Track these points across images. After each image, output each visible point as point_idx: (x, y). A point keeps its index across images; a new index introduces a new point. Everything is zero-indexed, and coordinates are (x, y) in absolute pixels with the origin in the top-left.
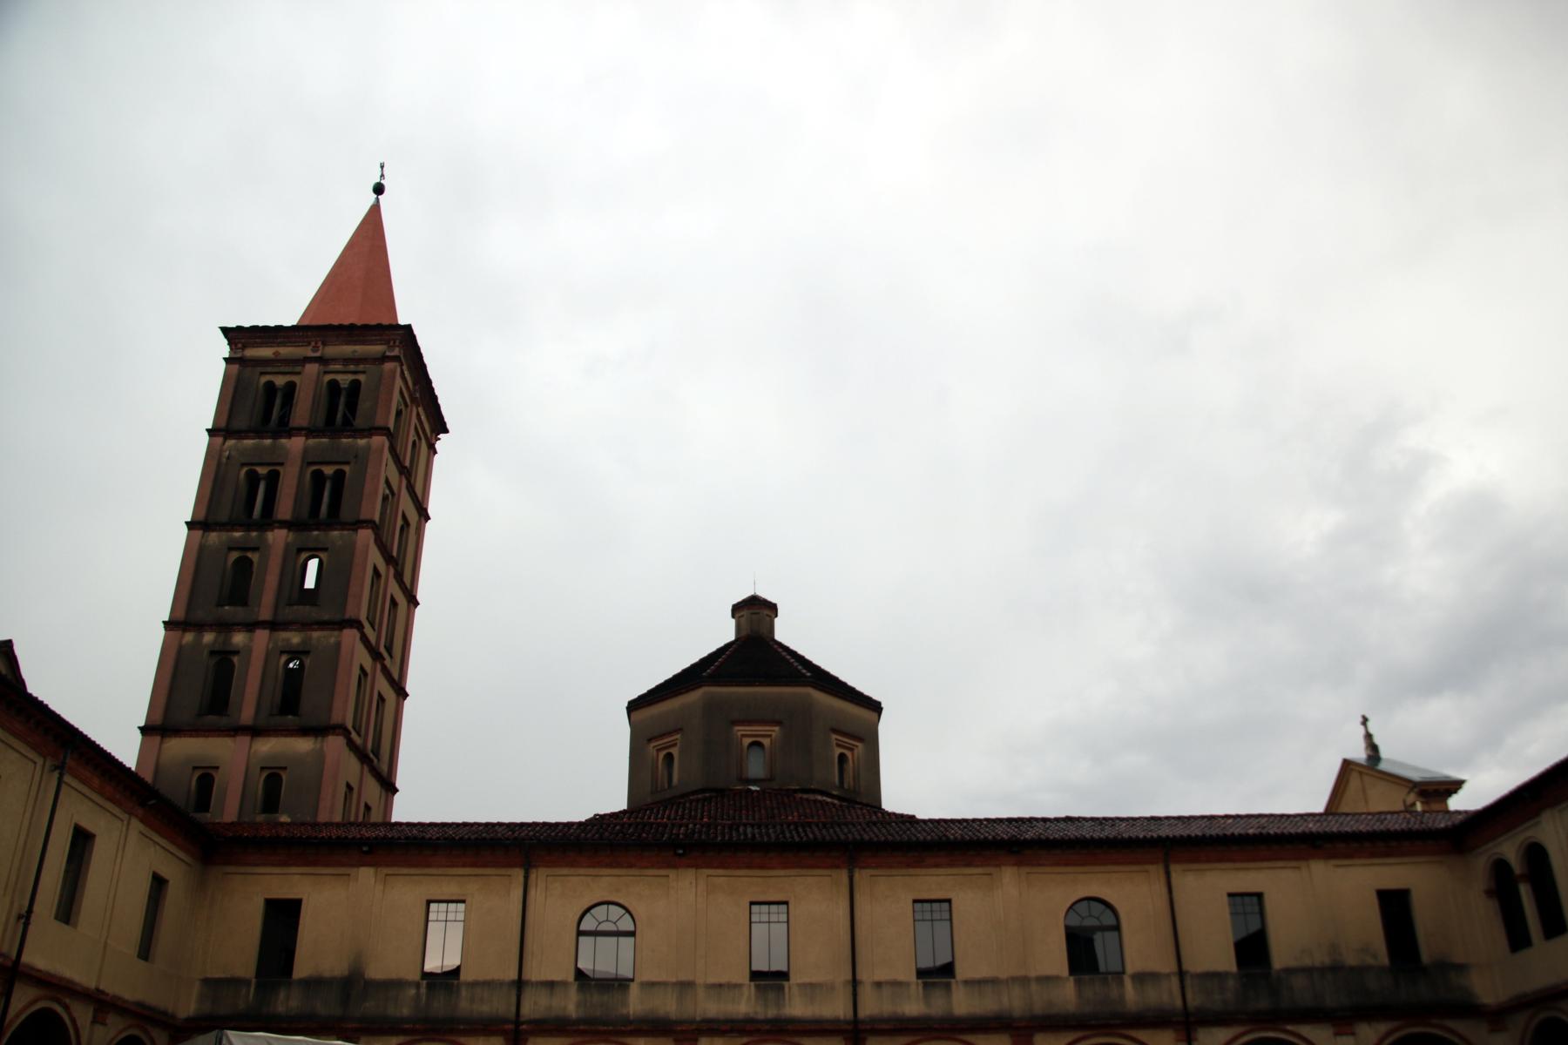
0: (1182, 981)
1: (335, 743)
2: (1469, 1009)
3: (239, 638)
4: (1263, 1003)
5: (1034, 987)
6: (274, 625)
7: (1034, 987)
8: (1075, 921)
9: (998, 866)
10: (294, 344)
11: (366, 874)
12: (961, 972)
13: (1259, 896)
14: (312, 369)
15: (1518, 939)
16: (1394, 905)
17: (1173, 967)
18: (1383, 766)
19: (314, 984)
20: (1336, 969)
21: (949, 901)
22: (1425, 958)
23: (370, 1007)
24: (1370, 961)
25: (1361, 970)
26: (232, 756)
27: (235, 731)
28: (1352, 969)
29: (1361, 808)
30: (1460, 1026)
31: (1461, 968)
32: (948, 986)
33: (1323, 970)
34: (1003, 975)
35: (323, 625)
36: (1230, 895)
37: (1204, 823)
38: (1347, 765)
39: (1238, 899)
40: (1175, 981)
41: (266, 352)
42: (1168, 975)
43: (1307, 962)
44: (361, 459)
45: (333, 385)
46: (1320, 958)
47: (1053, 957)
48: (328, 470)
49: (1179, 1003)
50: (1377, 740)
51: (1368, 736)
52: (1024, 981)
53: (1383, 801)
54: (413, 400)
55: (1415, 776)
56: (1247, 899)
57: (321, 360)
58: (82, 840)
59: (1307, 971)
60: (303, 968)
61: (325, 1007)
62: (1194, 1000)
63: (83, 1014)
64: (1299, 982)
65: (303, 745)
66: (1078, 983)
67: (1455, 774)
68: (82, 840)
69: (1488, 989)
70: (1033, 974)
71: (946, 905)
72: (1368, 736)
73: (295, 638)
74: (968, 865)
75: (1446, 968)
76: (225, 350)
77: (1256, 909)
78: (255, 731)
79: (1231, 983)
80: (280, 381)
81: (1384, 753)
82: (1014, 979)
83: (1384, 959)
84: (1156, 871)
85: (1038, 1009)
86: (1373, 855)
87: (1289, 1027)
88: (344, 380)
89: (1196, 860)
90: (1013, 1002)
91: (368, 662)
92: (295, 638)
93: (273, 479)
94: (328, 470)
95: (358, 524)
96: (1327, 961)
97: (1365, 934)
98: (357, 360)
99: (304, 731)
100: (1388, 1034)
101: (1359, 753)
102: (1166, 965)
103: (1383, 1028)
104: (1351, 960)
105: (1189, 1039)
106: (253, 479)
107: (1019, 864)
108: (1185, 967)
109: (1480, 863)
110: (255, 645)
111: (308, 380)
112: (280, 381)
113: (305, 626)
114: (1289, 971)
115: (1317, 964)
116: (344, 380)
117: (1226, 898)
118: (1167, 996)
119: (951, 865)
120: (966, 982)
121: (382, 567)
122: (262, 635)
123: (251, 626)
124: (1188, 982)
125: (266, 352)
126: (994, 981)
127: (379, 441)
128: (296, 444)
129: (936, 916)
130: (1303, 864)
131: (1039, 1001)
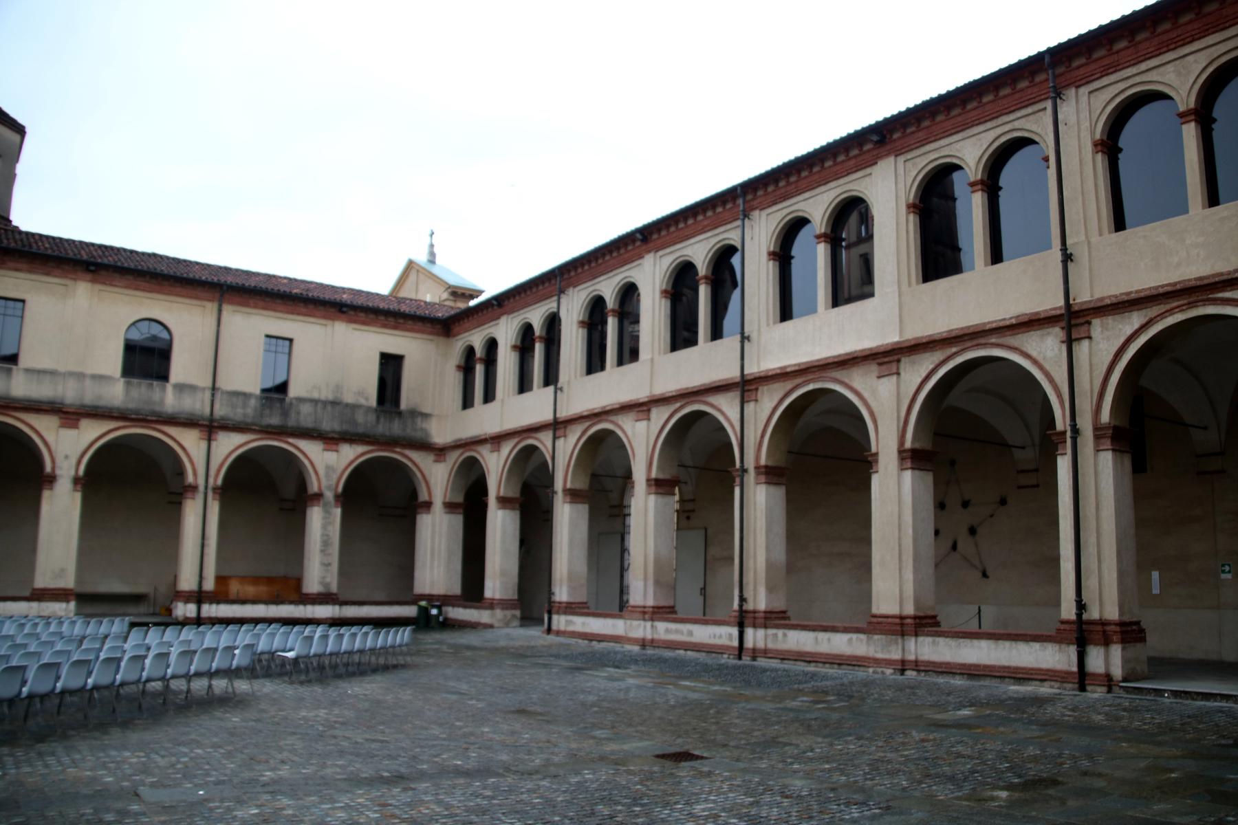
0: (213, 395)
2: (424, 446)
4: (275, 420)
5: (88, 382)
7: (88, 382)
8: (135, 336)
9: (75, 279)
12: (25, 361)
13: (291, 340)
15: (467, 403)
16: (391, 364)
17: (208, 383)
18: (435, 270)
20: (334, 403)
21: (23, 301)
22: (404, 405)
24: (363, 401)
25: (354, 407)
28: (347, 405)
29: (413, 296)
30: (415, 455)
31: (426, 416)
32: (9, 371)
33: (325, 403)
34: (61, 369)
36: (267, 336)
37: (302, 286)
38: (411, 265)
39: (274, 341)
40: (208, 394)
42: (204, 389)
43: (315, 395)
46: (327, 394)
47: (111, 360)
49: (207, 411)
50: (436, 250)
51: (432, 246)
52: (80, 376)
53: (430, 295)
55: (452, 281)
56: (280, 342)
59: (315, 402)
62: (221, 411)
64: (306, 409)
66: (128, 384)
67: (479, 286)
69: (440, 434)
70: (89, 371)
71: (20, 304)
72: (432, 246)
74: (48, 274)
75: (415, 414)
77: (287, 350)
79: (253, 402)
81: (438, 260)
82: (71, 374)
83: (373, 402)
84: (211, 307)
85: (89, 399)
86: (385, 326)
87: (291, 440)
89: (247, 305)
90: (69, 393)
96: (330, 397)
97: (363, 384)
100: (363, 454)
101: (421, 258)
102: (205, 381)
103: (360, 449)
104: (349, 399)
105: (209, 440)
107: (94, 281)
108: (218, 385)
109: (457, 346)
114: (301, 400)
115: (323, 397)
117: (263, 338)
118: (198, 405)
119: (30, 271)
120: (27, 370)
124: (218, 396)
126: (53, 373)
129: (10, 312)
130: (329, 322)
131: (90, 394)
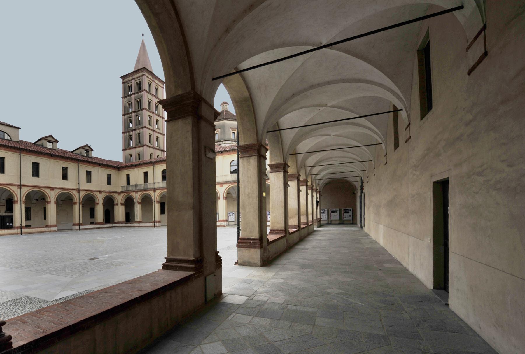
1: (145, 147)
3: (131, 133)
6: (135, 130)
10: (130, 77)
11: (136, 169)
14: (133, 81)
19: (132, 186)
23: (138, 188)
26: (133, 152)
27: (133, 148)
35: (141, 128)
41: (126, 80)
44: (142, 96)
45: (137, 83)
48: (139, 100)
54: (153, 81)
57: (134, 79)
58: (89, 173)
60: (131, 184)
61: (134, 189)
63: (97, 194)
65: (141, 149)
68: (89, 173)
73: (138, 131)
76: (121, 81)
78: (135, 148)
80: (130, 85)
88: (138, 81)
91: (151, 132)
92: (138, 131)
93: (132, 103)
94: (139, 100)
95: (143, 109)
98: (139, 77)
99: (141, 146)
106: (129, 104)
110: (133, 133)
111: (133, 83)
112: (130, 85)
113: (139, 129)
116: (138, 81)
121: (151, 114)
122: (134, 131)
123: (132, 130)
125: (126, 80)
127: (144, 92)
128: (133, 96)
